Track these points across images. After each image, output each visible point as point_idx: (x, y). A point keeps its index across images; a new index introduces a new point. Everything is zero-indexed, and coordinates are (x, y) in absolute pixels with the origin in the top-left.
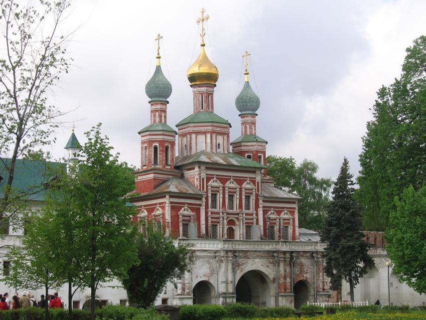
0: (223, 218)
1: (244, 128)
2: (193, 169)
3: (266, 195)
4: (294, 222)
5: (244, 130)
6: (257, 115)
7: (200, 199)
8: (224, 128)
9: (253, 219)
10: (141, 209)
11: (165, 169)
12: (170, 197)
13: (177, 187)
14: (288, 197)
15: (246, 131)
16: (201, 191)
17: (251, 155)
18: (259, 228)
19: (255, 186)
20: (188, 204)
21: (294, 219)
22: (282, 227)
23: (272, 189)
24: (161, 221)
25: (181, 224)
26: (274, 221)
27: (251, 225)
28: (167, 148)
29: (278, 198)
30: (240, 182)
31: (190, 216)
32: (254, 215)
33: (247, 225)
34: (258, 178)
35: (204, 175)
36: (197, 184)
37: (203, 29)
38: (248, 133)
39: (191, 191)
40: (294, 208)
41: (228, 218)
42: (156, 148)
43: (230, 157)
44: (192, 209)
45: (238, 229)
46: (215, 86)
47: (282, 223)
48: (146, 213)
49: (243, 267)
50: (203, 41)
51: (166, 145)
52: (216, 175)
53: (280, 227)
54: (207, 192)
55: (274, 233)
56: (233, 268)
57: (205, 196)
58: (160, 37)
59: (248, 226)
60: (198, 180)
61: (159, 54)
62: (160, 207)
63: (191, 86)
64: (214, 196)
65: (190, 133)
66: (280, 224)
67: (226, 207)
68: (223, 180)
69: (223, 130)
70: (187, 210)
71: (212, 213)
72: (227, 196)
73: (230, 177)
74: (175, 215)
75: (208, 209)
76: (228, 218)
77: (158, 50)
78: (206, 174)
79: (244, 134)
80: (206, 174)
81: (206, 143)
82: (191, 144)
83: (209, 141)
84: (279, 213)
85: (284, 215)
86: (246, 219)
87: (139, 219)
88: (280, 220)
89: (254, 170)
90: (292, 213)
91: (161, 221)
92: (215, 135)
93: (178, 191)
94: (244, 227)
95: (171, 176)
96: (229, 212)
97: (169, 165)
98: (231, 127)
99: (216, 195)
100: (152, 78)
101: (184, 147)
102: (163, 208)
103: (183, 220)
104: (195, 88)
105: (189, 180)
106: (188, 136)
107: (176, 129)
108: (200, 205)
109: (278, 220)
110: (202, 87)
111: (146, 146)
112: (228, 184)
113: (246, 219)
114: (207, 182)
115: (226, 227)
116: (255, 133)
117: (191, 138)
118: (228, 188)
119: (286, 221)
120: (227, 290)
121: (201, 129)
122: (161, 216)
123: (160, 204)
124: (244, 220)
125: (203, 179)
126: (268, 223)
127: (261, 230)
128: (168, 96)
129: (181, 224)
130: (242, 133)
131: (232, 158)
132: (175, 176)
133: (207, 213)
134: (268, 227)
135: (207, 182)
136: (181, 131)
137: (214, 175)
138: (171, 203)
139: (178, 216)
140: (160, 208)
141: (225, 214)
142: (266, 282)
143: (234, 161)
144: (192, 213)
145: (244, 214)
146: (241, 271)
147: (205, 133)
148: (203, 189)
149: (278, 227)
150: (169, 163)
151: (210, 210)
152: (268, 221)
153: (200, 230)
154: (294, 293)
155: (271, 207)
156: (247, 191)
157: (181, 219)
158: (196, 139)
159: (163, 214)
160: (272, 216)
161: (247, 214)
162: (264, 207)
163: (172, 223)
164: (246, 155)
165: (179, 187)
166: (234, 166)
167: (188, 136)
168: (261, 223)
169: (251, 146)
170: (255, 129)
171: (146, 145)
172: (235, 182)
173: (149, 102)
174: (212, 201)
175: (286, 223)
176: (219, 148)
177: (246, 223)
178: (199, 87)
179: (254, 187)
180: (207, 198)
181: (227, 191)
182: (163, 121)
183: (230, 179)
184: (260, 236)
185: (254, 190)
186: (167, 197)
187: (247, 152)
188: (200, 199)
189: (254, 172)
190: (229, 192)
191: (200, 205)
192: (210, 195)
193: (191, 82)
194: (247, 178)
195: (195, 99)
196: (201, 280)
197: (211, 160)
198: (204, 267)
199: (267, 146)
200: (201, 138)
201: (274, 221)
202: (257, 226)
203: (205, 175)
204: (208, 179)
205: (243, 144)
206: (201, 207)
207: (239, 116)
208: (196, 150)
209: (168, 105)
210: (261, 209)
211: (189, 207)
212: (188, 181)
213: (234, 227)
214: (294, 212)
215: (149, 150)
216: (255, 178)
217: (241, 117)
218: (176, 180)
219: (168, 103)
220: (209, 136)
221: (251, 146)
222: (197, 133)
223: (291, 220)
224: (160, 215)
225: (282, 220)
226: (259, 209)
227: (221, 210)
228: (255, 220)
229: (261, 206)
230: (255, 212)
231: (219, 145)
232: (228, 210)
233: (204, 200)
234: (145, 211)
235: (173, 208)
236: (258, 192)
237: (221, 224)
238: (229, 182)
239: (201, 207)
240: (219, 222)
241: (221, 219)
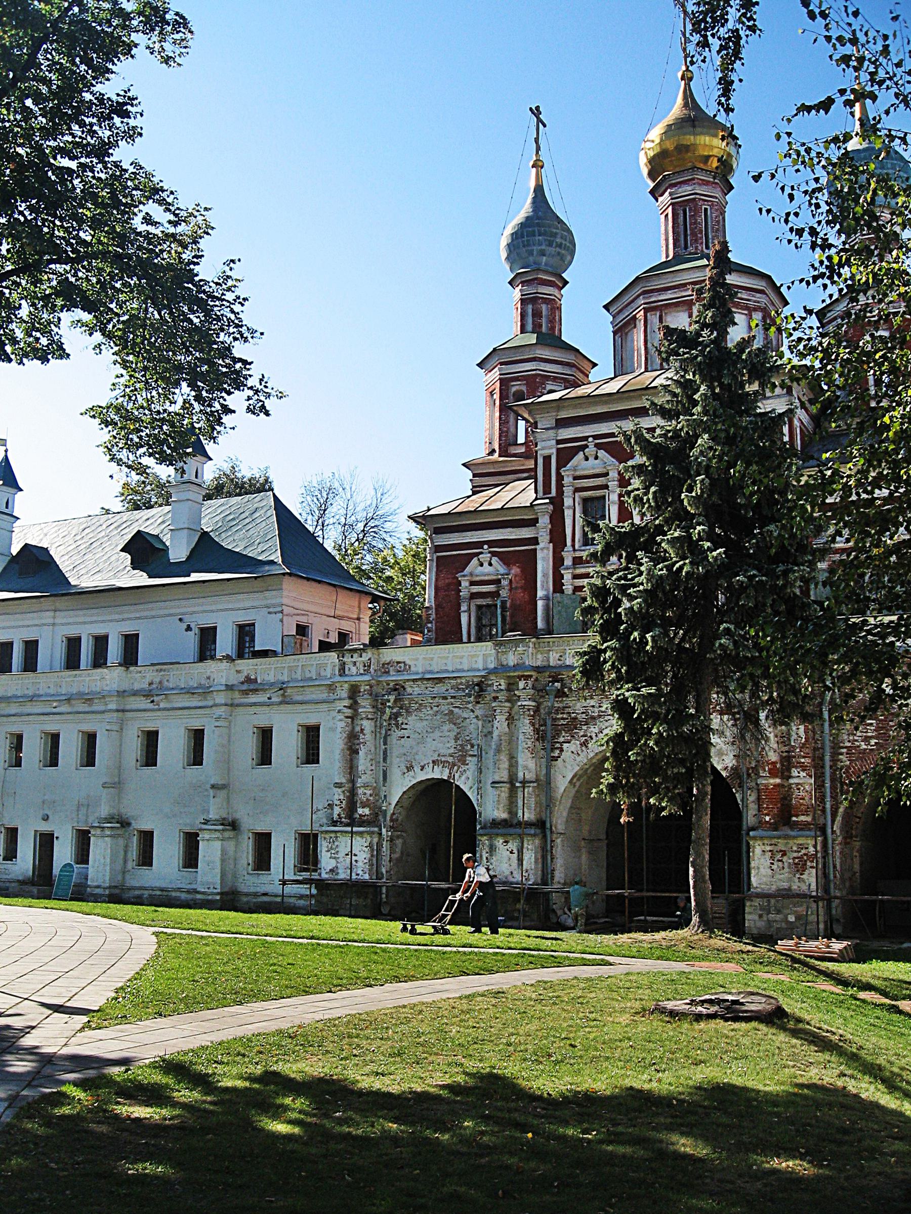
7: (533, 522)
20: (491, 543)
31: (497, 582)
49: (594, 730)
51: (514, 389)
52: (595, 437)
56: (540, 736)
74: (449, 585)
80: (559, 442)
103: (473, 596)
108: (535, 541)
114: (562, 464)
120: (512, 812)
125: (547, 459)
133: (558, 561)
135: (562, 464)
146: (584, 744)
188: (533, 522)
191: (535, 541)
196: (422, 776)
198: (437, 734)
203: (554, 442)
204: (565, 456)
206: (538, 547)
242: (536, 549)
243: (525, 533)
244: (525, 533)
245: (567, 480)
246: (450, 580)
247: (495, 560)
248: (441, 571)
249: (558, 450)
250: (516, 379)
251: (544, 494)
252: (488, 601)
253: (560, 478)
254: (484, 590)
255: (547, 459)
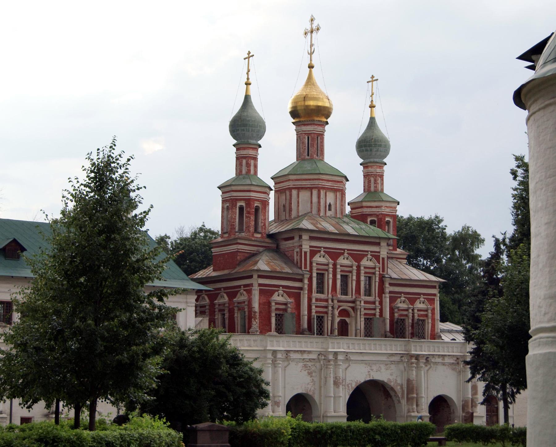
0: (333, 307)
1: (367, 182)
2: (292, 238)
3: (394, 276)
4: (433, 314)
5: (367, 184)
6: (386, 164)
7: (301, 280)
8: (338, 182)
9: (375, 309)
10: (219, 293)
11: (253, 239)
12: (260, 277)
13: (268, 264)
14: (425, 278)
15: (369, 187)
16: (303, 269)
17: (376, 219)
18: (384, 320)
19: (379, 264)
20: (284, 287)
21: (433, 310)
22: (416, 321)
23: (402, 267)
24: (246, 310)
25: (273, 314)
26: (405, 313)
27: (371, 317)
28: (257, 209)
29: (411, 280)
30: (358, 257)
31: (286, 304)
32: (377, 303)
33: (366, 317)
34: (384, 252)
35: (306, 247)
36: (297, 260)
37: (312, 45)
38: (372, 189)
39: (287, 270)
40: (435, 295)
41: (339, 307)
42: (241, 208)
43: (344, 222)
44: (289, 295)
45: (354, 323)
46: (327, 123)
47: (416, 315)
48: (226, 299)
50: (311, 60)
51: (256, 205)
52: (324, 248)
53: (413, 320)
54: (311, 271)
55: (405, 329)
57: (308, 276)
58: (249, 56)
59: (368, 319)
60: (299, 255)
61: (248, 79)
62: (244, 290)
63: (293, 123)
64: (321, 277)
65: (290, 189)
66: (413, 316)
67: (338, 292)
68: (334, 255)
69: (336, 186)
70: (282, 296)
71: (317, 300)
72: (339, 277)
73: (344, 250)
74: (265, 302)
75: (311, 295)
76: (339, 307)
77: (247, 74)
78: (311, 247)
79: (366, 190)
80: (311, 247)
81: (311, 203)
82: (291, 204)
83: (315, 199)
84: (412, 301)
85: (419, 305)
86: (365, 309)
87: (217, 306)
88: (413, 310)
89: (377, 241)
90: (432, 301)
91: (246, 310)
92: (324, 191)
93: (269, 269)
94: (363, 319)
95: (261, 249)
96: (342, 299)
97: (259, 233)
98: (347, 180)
99: (323, 274)
100: (238, 113)
101: (282, 208)
102: (249, 292)
103: (277, 309)
104: (299, 126)
105: (287, 253)
106: (288, 193)
107: (271, 184)
108: (301, 289)
109: (410, 311)
110: (308, 125)
111: (228, 206)
112: (342, 261)
113: (365, 309)
115: (337, 320)
116: (382, 190)
117: (291, 195)
118: (341, 266)
119: (422, 313)
121: (304, 183)
122: (246, 303)
123: (245, 286)
124: (362, 309)
125: (305, 253)
126: (396, 315)
127: (385, 325)
128: (260, 138)
129: (273, 314)
130: (364, 190)
131: (348, 224)
132: (268, 249)
133: (310, 300)
134: (395, 320)
136: (278, 186)
137: (320, 247)
138: (260, 285)
139: (269, 303)
140: (245, 292)
141: (335, 302)
142: (391, 397)
143: (350, 229)
144: (289, 300)
145: (362, 302)
147: (311, 189)
148: (305, 267)
149: (410, 321)
150: (260, 230)
151: (315, 295)
152: (397, 313)
153: (300, 322)
154: (429, 413)
155: (400, 293)
156: (368, 270)
157: (273, 308)
158: (298, 197)
159: (250, 302)
160: (403, 306)
161: (366, 302)
162: (390, 292)
163: (260, 312)
164: (369, 220)
165: (271, 264)
166: (349, 235)
167: (288, 193)
168: (387, 315)
169: (377, 207)
170: (382, 184)
171: (228, 205)
172: (350, 258)
173: (234, 145)
174: (318, 283)
175: (422, 315)
176: (330, 209)
177: (365, 314)
178: (305, 125)
179: (377, 264)
180: (310, 279)
181: (338, 270)
182: (252, 172)
183: (343, 254)
184: (383, 333)
185: (377, 269)
186: (255, 276)
187: (371, 215)
188: (301, 280)
189: (378, 244)
190: (342, 271)
191: (301, 289)
192: (315, 275)
193: (294, 119)
194: (367, 251)
195: (299, 141)
197: (317, 227)
199: (398, 207)
200: (304, 195)
201: (405, 313)
202: (382, 319)
203: (308, 247)
204: (313, 253)
205: (364, 204)
206: (302, 292)
207: (361, 164)
208: (298, 212)
209: (260, 149)
210: (388, 295)
211: (284, 291)
212: (285, 254)
213: (347, 320)
214: (434, 300)
215: (232, 212)
216: (379, 252)
217: (364, 167)
218: (268, 254)
219: (260, 146)
220: (315, 192)
221: (377, 207)
222: (299, 189)
223: (430, 311)
224: (244, 302)
225: (416, 311)
226: (384, 295)
227: (330, 296)
228: (378, 310)
229: (387, 290)
230: (377, 299)
231: (330, 205)
232: (339, 296)
233: (306, 281)
234: (225, 296)
235: (261, 292)
236: (383, 271)
237: (330, 315)
238: (342, 257)
239: (302, 292)
240: (326, 313)
241: (330, 308)
242: (300, 293)
243: (297, 284)
244: (297, 284)
245: (314, 264)
246: (265, 301)
247: (285, 295)
248: (261, 296)
249: (310, 250)
250: (258, 200)
251: (304, 268)
252: (281, 312)
253: (311, 263)
254: (280, 307)
255: (305, 253)
